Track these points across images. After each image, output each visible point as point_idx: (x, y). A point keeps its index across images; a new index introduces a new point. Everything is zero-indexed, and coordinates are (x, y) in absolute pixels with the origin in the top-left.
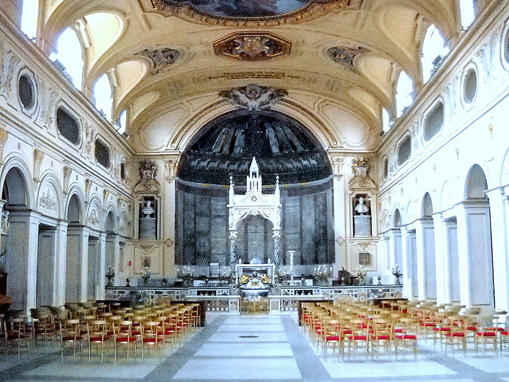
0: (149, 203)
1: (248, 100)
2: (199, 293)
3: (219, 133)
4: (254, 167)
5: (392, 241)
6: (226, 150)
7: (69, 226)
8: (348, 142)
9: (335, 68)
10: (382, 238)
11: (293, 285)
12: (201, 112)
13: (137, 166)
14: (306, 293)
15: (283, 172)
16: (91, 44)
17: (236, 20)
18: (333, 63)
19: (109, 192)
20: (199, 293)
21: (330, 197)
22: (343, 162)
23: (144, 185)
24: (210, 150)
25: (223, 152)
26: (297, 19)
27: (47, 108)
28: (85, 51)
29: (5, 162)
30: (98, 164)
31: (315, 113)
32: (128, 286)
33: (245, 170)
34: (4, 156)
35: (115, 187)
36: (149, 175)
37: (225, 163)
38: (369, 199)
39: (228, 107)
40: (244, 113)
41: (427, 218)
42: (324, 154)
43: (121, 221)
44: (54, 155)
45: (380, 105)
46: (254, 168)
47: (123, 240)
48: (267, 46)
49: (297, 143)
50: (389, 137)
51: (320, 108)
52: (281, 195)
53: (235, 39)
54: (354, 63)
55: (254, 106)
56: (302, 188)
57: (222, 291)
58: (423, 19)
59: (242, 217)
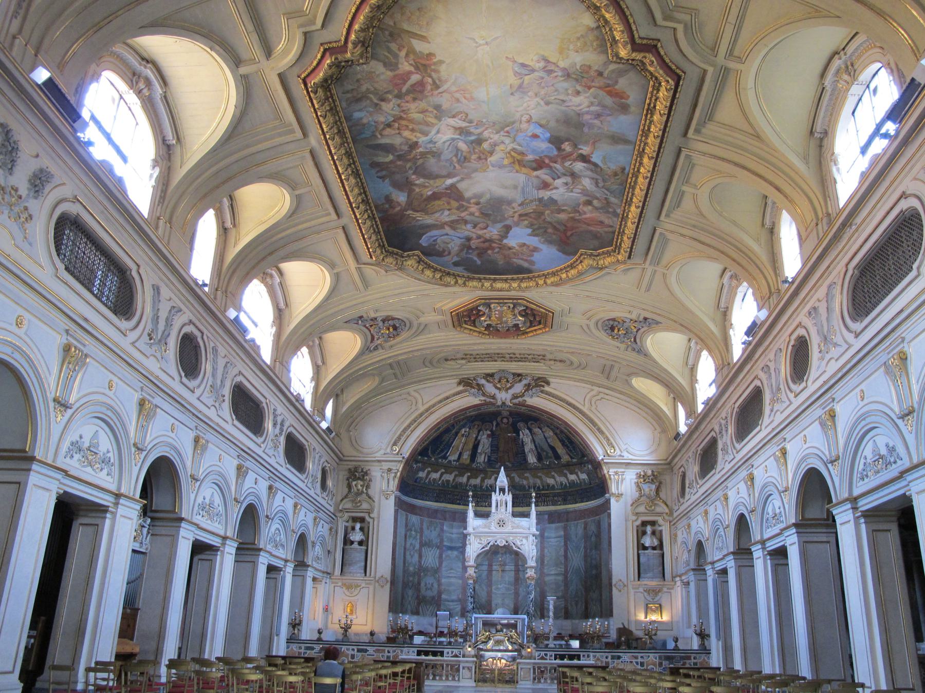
0: (358, 526)
1: (497, 392)
2: (419, 653)
3: (457, 434)
4: (502, 479)
5: (692, 585)
6: (466, 456)
7: (238, 549)
8: (630, 450)
9: (611, 348)
10: (679, 583)
11: (553, 646)
12: (434, 406)
13: (343, 475)
14: (571, 657)
15: (543, 490)
16: (287, 305)
17: (480, 279)
18: (609, 340)
19: (302, 506)
20: (419, 653)
21: (607, 524)
22: (624, 477)
23: (353, 501)
24: (445, 457)
26: (561, 279)
27: (219, 382)
28: (280, 315)
29: (149, 448)
30: (288, 466)
31: (585, 410)
32: (319, 639)
33: (491, 486)
34: (148, 439)
35: (311, 501)
36: (360, 487)
37: (463, 476)
38: (660, 528)
39: (470, 400)
40: (492, 409)
41: (743, 552)
42: (597, 465)
43: (318, 548)
44: (224, 446)
45: (674, 398)
46: (503, 482)
47: (319, 575)
48: (522, 316)
49: (561, 450)
50: (686, 442)
51: (593, 403)
52: (537, 519)
53: (479, 306)
54: (638, 340)
55: (503, 399)
56: (567, 512)
57: (452, 652)
58: (731, 277)
59: (483, 548)
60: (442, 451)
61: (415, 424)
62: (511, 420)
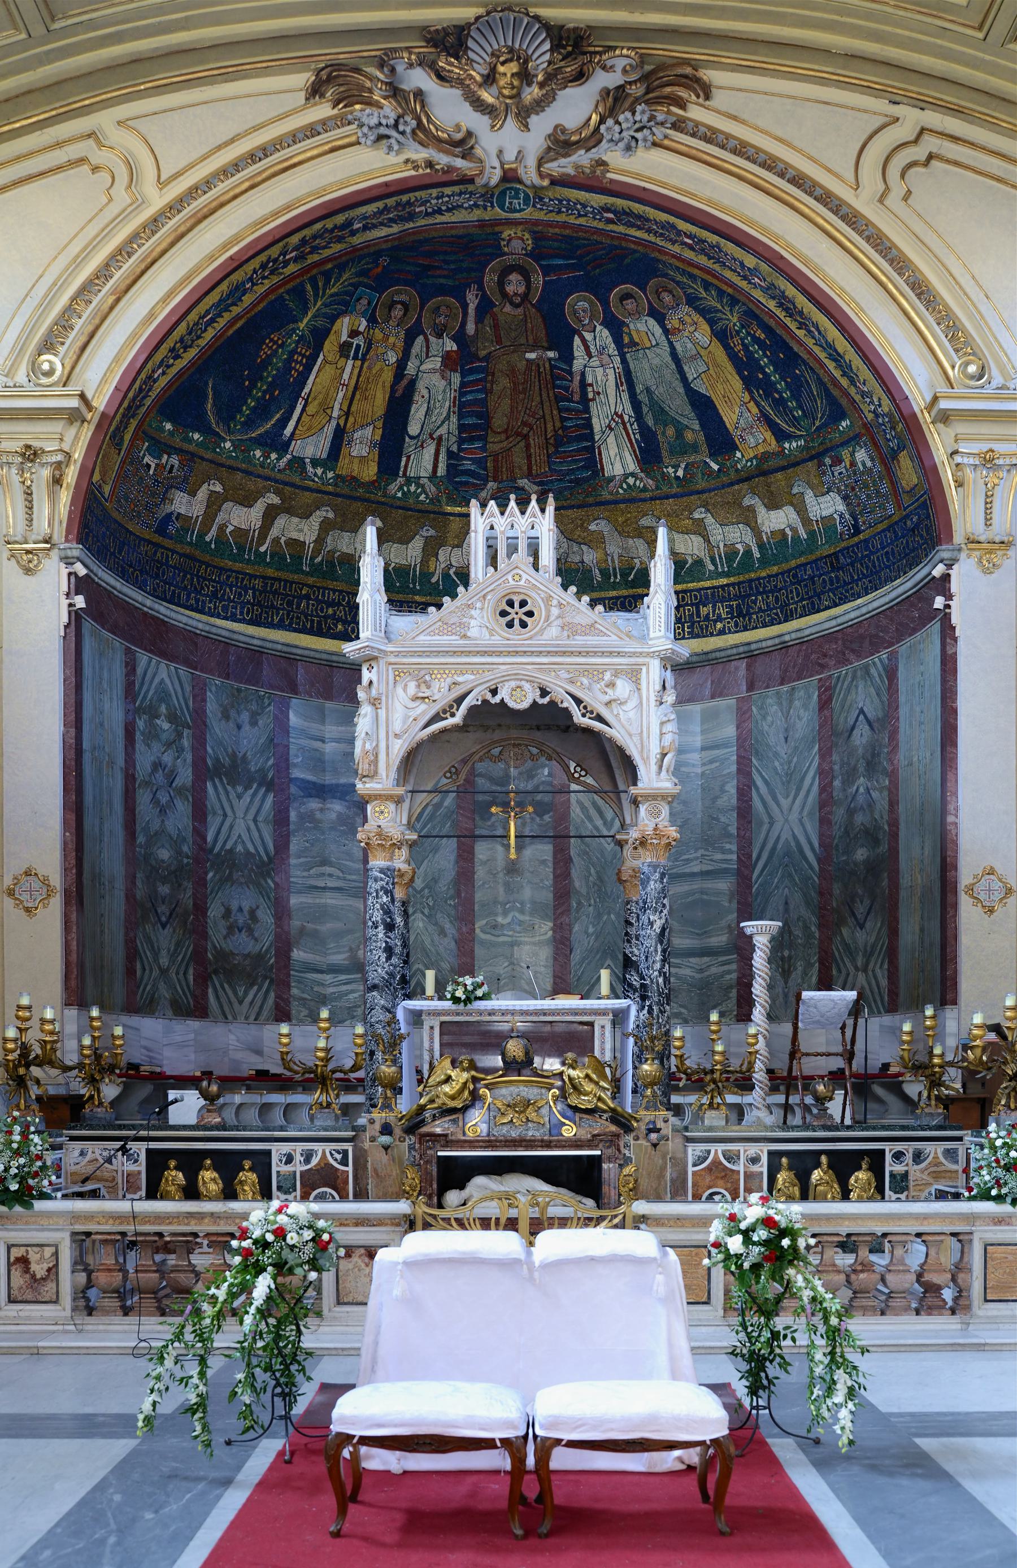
3: (319, 336)
25: (344, 467)
55: (510, 156)
56: (751, 655)
60: (263, 411)
61: (129, 265)
62: (538, 280)
